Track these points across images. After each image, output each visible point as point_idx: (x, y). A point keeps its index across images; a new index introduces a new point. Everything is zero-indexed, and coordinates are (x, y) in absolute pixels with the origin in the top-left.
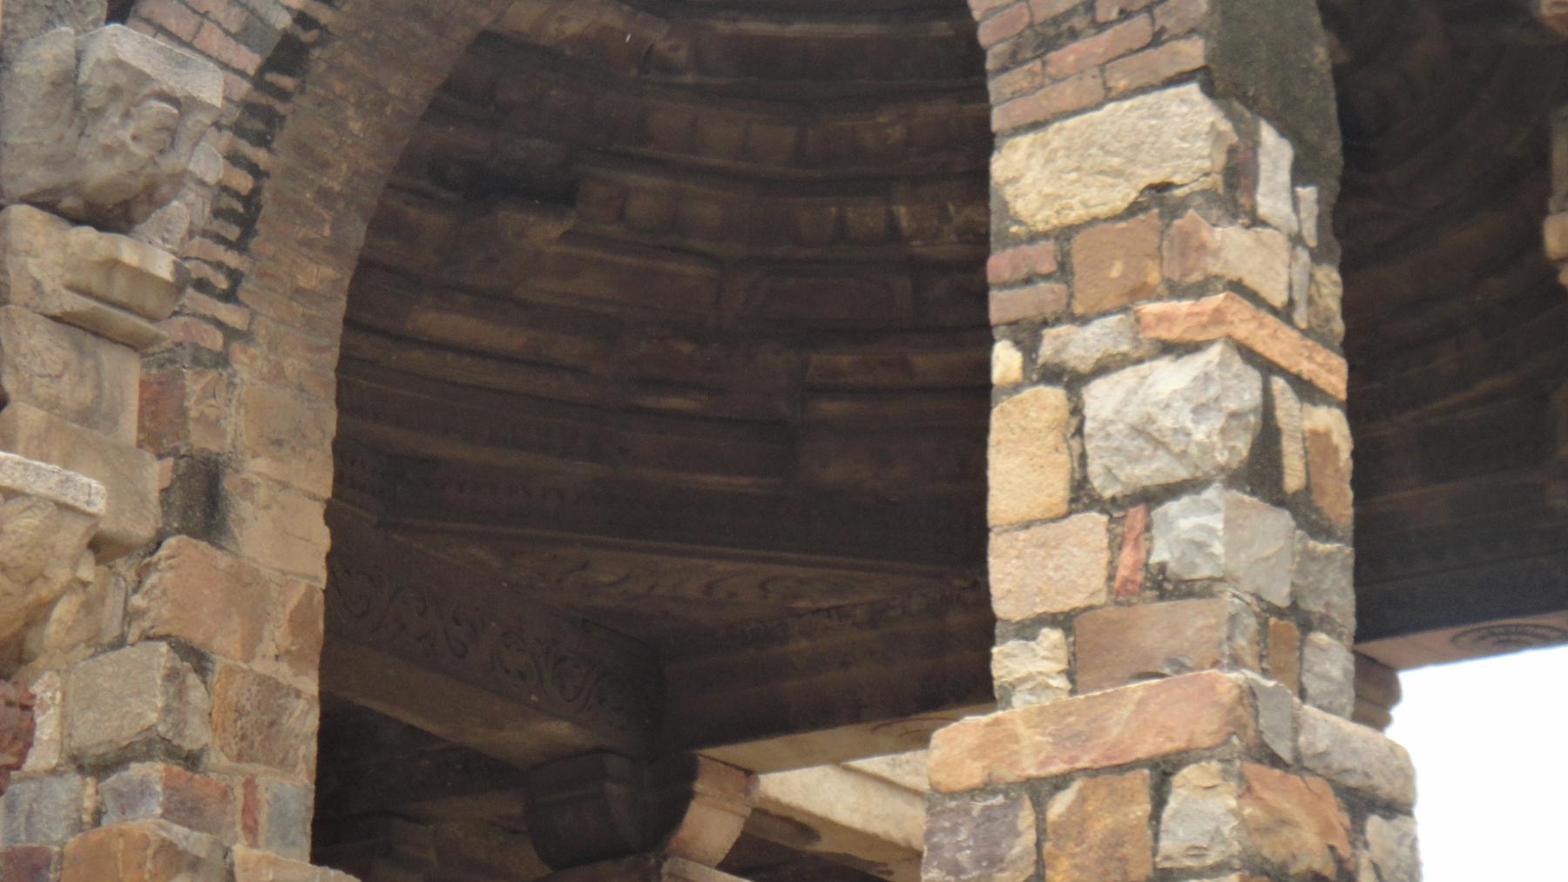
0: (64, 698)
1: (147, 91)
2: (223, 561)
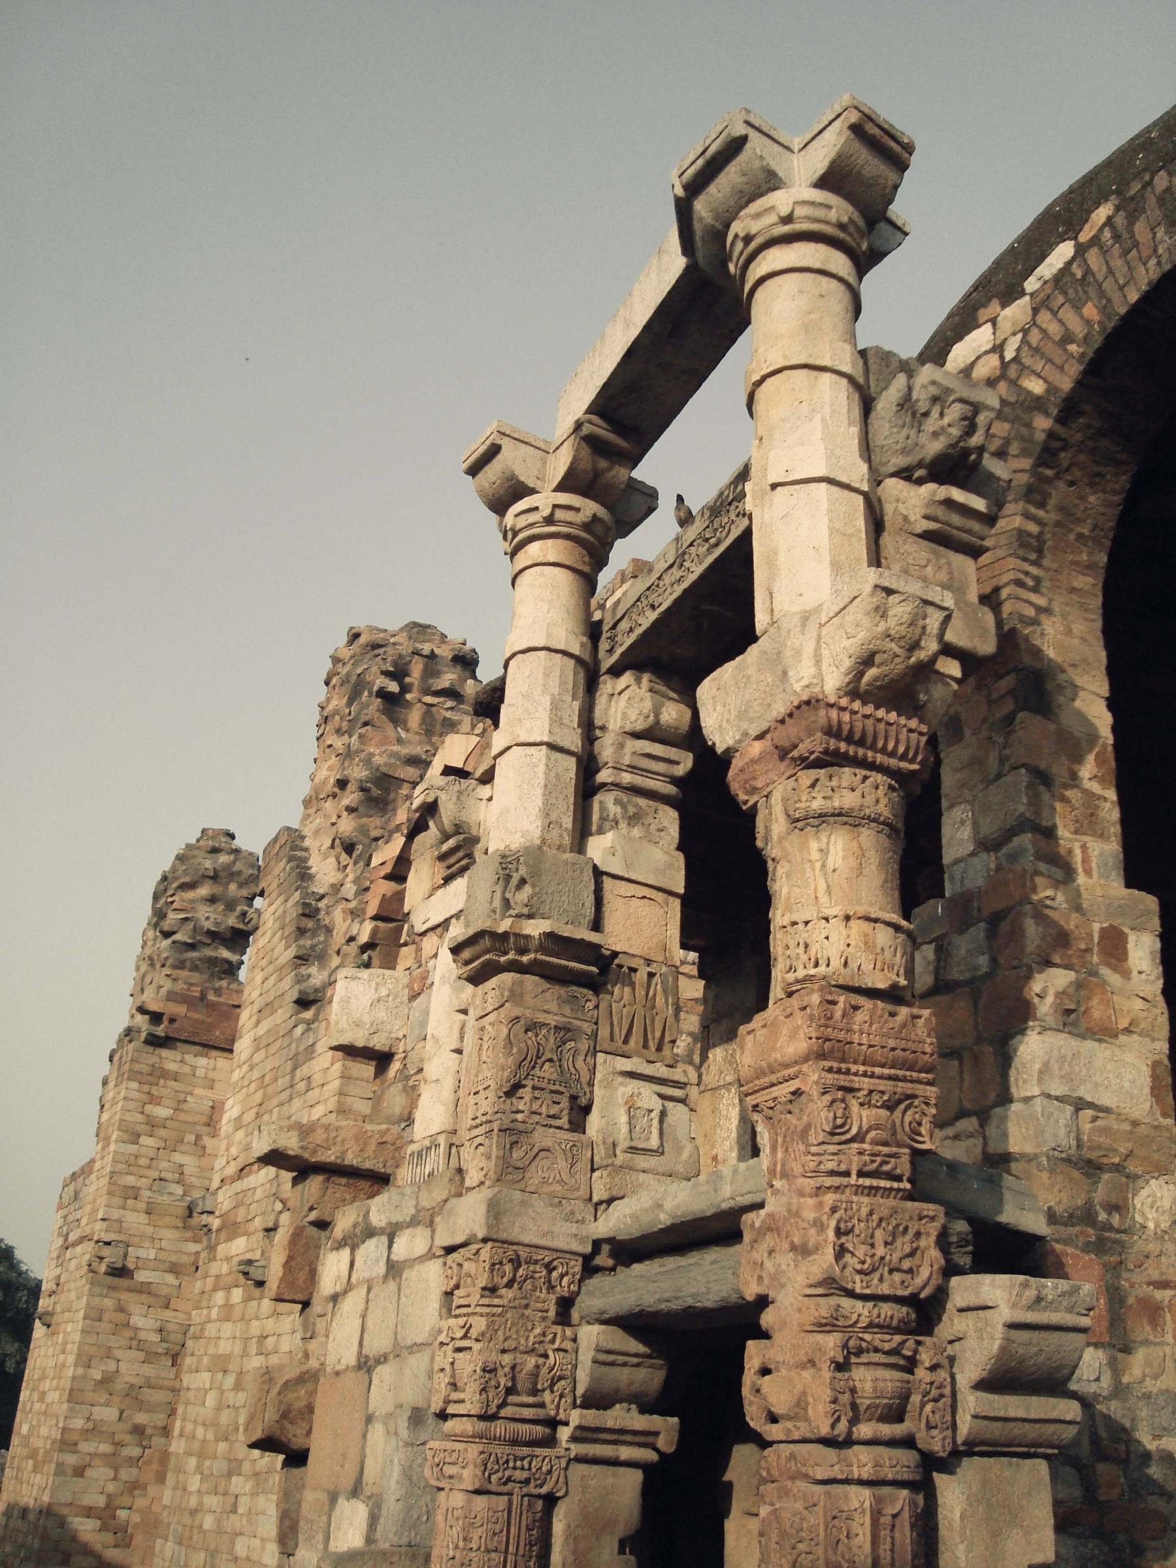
0: (973, 815)
1: (952, 398)
2: (1052, 727)
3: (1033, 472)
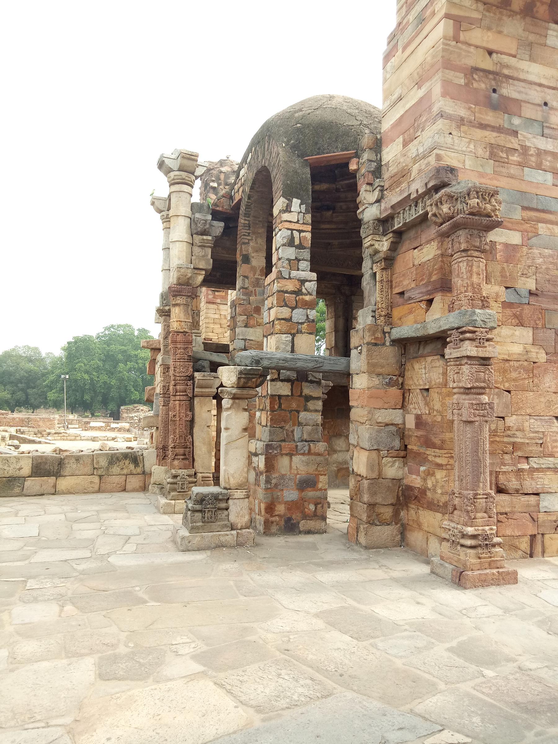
2: (249, 266)
3: (245, 210)
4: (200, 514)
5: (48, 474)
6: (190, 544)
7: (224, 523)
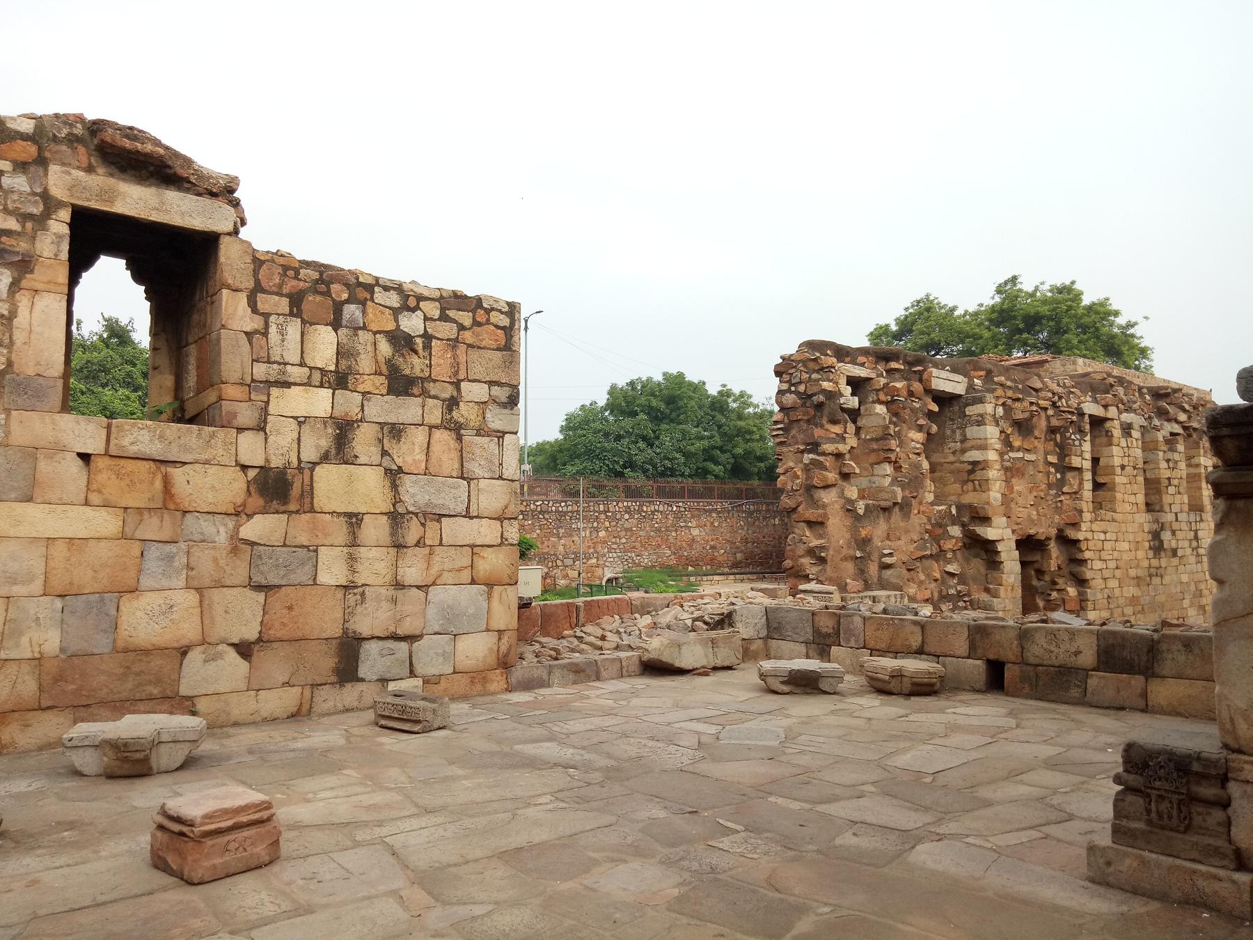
4: (1140, 801)
5: (1129, 668)
6: (1111, 869)
7: (1211, 841)
